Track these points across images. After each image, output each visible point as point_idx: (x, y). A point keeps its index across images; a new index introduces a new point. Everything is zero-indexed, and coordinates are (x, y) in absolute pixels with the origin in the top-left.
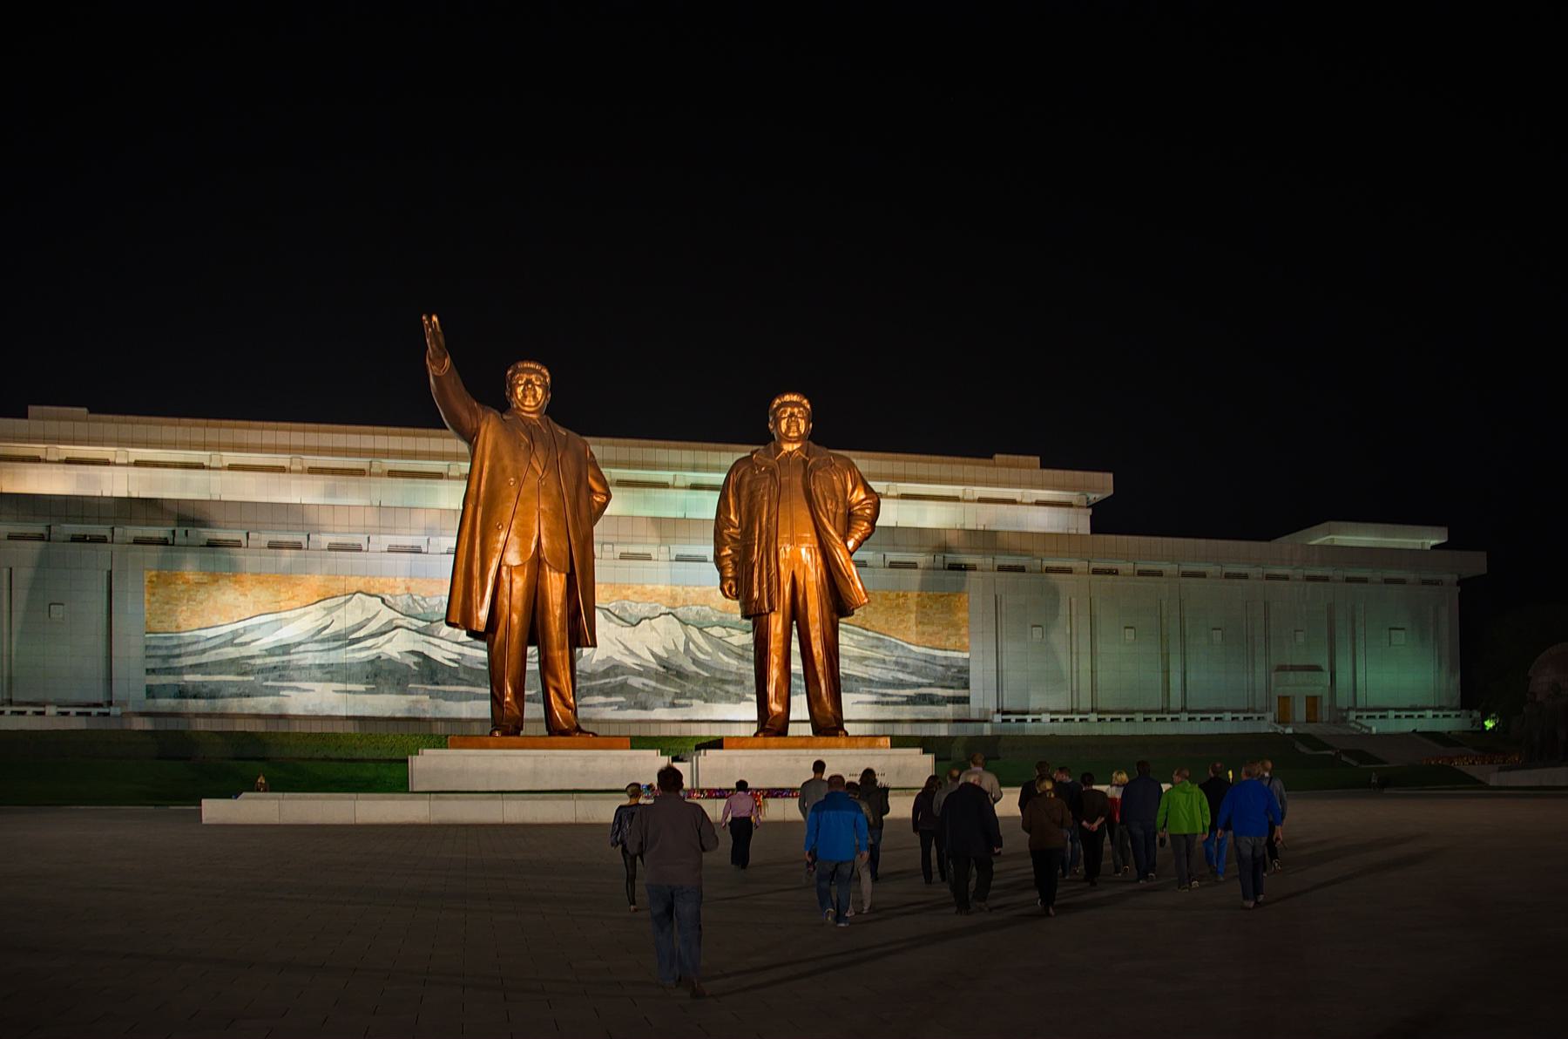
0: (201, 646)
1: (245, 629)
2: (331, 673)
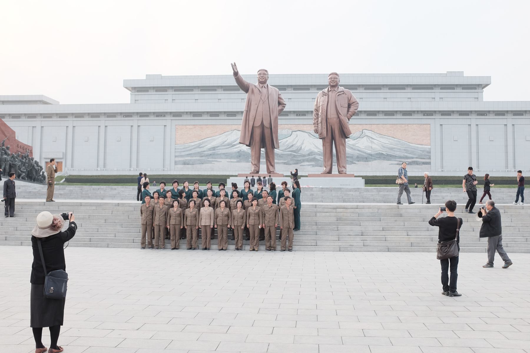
0: (190, 148)
2: (227, 156)
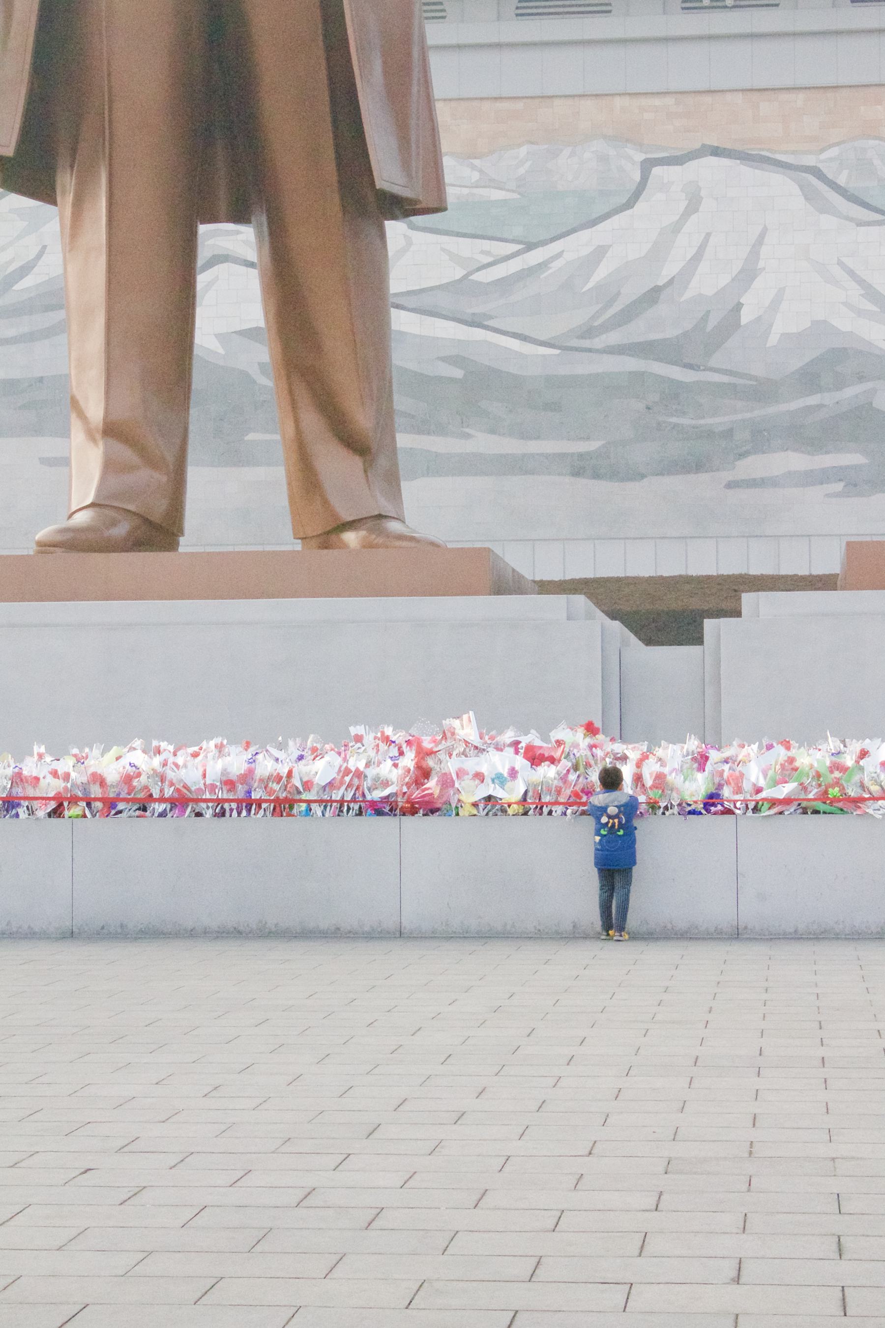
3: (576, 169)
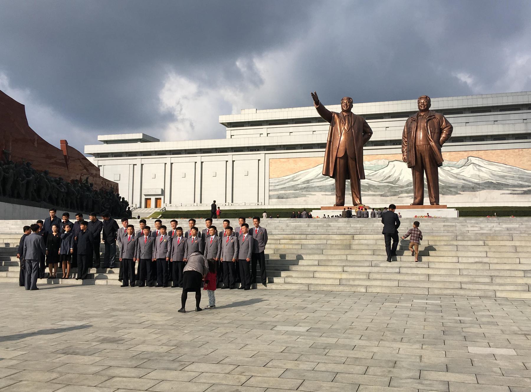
0: (284, 182)
1: (297, 176)
3: (381, 162)
